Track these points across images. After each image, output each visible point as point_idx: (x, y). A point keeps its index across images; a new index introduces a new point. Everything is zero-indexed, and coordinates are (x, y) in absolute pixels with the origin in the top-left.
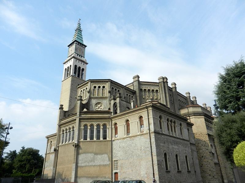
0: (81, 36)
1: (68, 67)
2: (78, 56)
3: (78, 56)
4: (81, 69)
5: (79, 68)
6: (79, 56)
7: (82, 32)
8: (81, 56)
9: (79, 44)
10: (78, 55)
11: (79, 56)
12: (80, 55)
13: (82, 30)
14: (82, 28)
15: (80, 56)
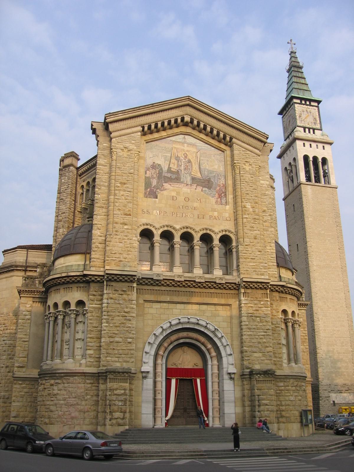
0: (302, 81)
1: (290, 164)
2: (305, 131)
3: (305, 131)
4: (320, 160)
5: (315, 158)
6: (307, 130)
7: (303, 70)
8: (314, 130)
9: (303, 102)
10: (305, 128)
11: (307, 130)
12: (309, 129)
13: (301, 64)
14: (301, 60)
15: (311, 131)
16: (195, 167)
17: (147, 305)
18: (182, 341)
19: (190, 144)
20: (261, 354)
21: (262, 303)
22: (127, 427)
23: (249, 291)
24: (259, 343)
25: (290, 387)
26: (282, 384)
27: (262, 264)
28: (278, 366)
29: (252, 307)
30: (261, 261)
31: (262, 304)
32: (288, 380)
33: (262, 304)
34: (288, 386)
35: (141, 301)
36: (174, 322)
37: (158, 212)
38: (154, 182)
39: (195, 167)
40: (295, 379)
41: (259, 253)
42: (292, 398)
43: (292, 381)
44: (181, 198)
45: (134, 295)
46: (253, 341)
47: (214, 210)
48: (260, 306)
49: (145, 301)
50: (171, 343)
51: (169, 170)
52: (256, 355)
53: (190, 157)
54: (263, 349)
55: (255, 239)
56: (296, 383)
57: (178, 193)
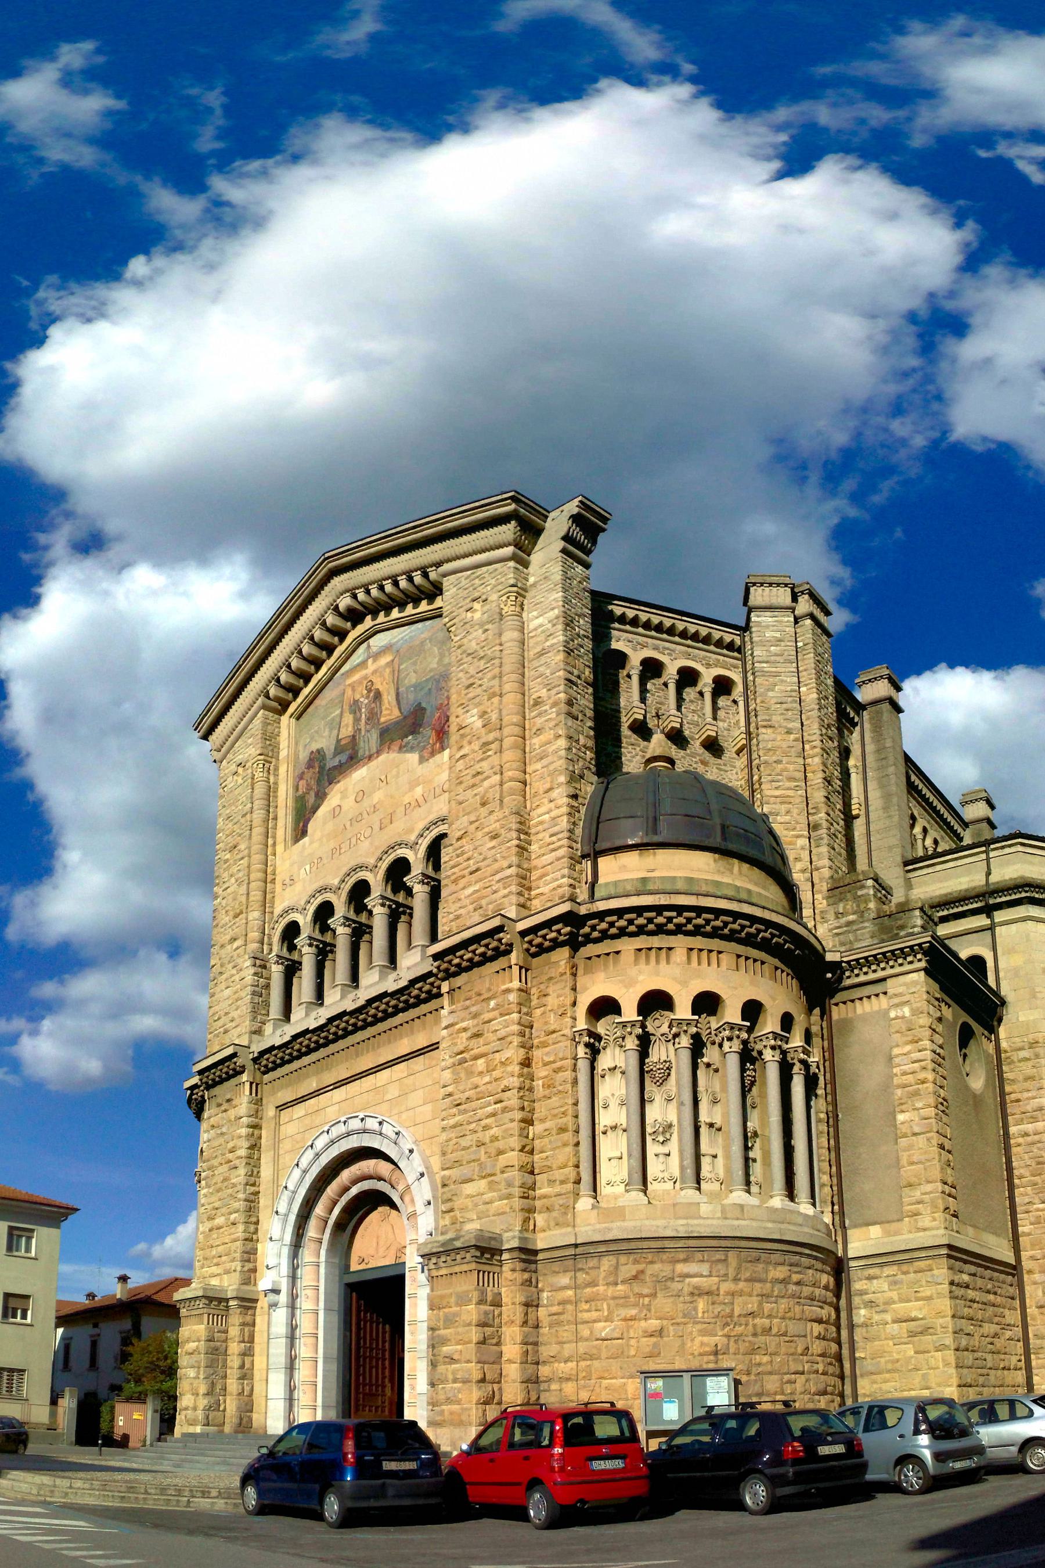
16: (389, 698)
17: (285, 1115)
18: (354, 1191)
19: (376, 656)
20: (483, 1183)
21: (492, 1003)
22: (198, 1429)
23: (459, 981)
24: (481, 1144)
25: (601, 1288)
26: (565, 1280)
27: (497, 877)
28: (555, 1214)
29: (465, 1030)
30: (496, 866)
31: (493, 1010)
32: (592, 1263)
33: (493, 1010)
34: (593, 1284)
35: (271, 1112)
36: (320, 1144)
37: (308, 867)
38: (311, 799)
39: (389, 698)
40: (629, 1252)
41: (493, 843)
42: (604, 1329)
43: (607, 1263)
44: (349, 804)
45: (243, 1103)
46: (464, 1142)
47: (413, 785)
48: (487, 1016)
49: (281, 1107)
50: (335, 1203)
51: (339, 750)
52: (469, 1189)
53: (378, 685)
54: (489, 1163)
55: (483, 804)
56: (628, 1269)
57: (344, 795)
